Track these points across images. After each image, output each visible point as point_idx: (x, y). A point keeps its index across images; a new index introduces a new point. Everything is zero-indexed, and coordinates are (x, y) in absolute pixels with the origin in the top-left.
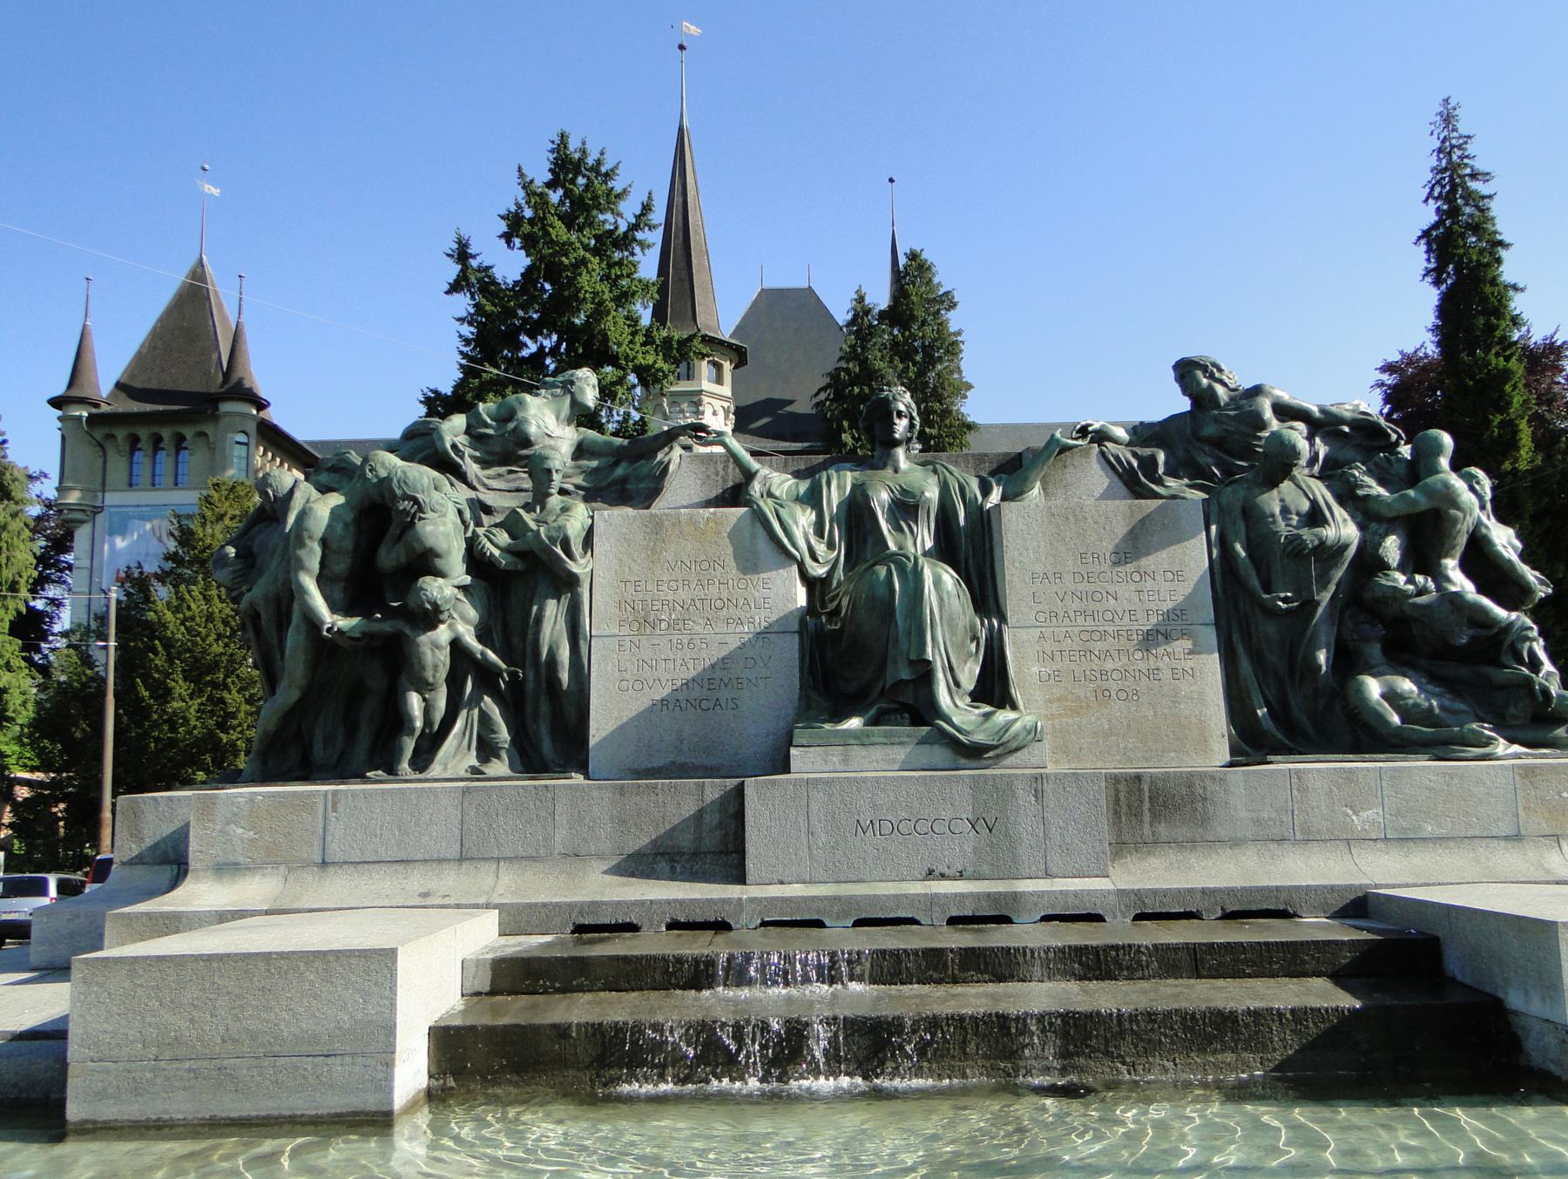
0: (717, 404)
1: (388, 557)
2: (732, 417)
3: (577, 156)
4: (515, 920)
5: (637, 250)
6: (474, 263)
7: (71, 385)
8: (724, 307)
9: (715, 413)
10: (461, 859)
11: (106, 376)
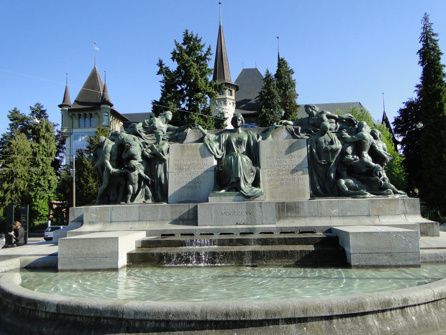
0: (231, 101)
1: (124, 156)
2: (235, 104)
3: (191, 36)
4: (149, 233)
5: (207, 61)
7: (63, 101)
8: (232, 75)
9: (230, 104)
10: (139, 221)
11: (72, 100)
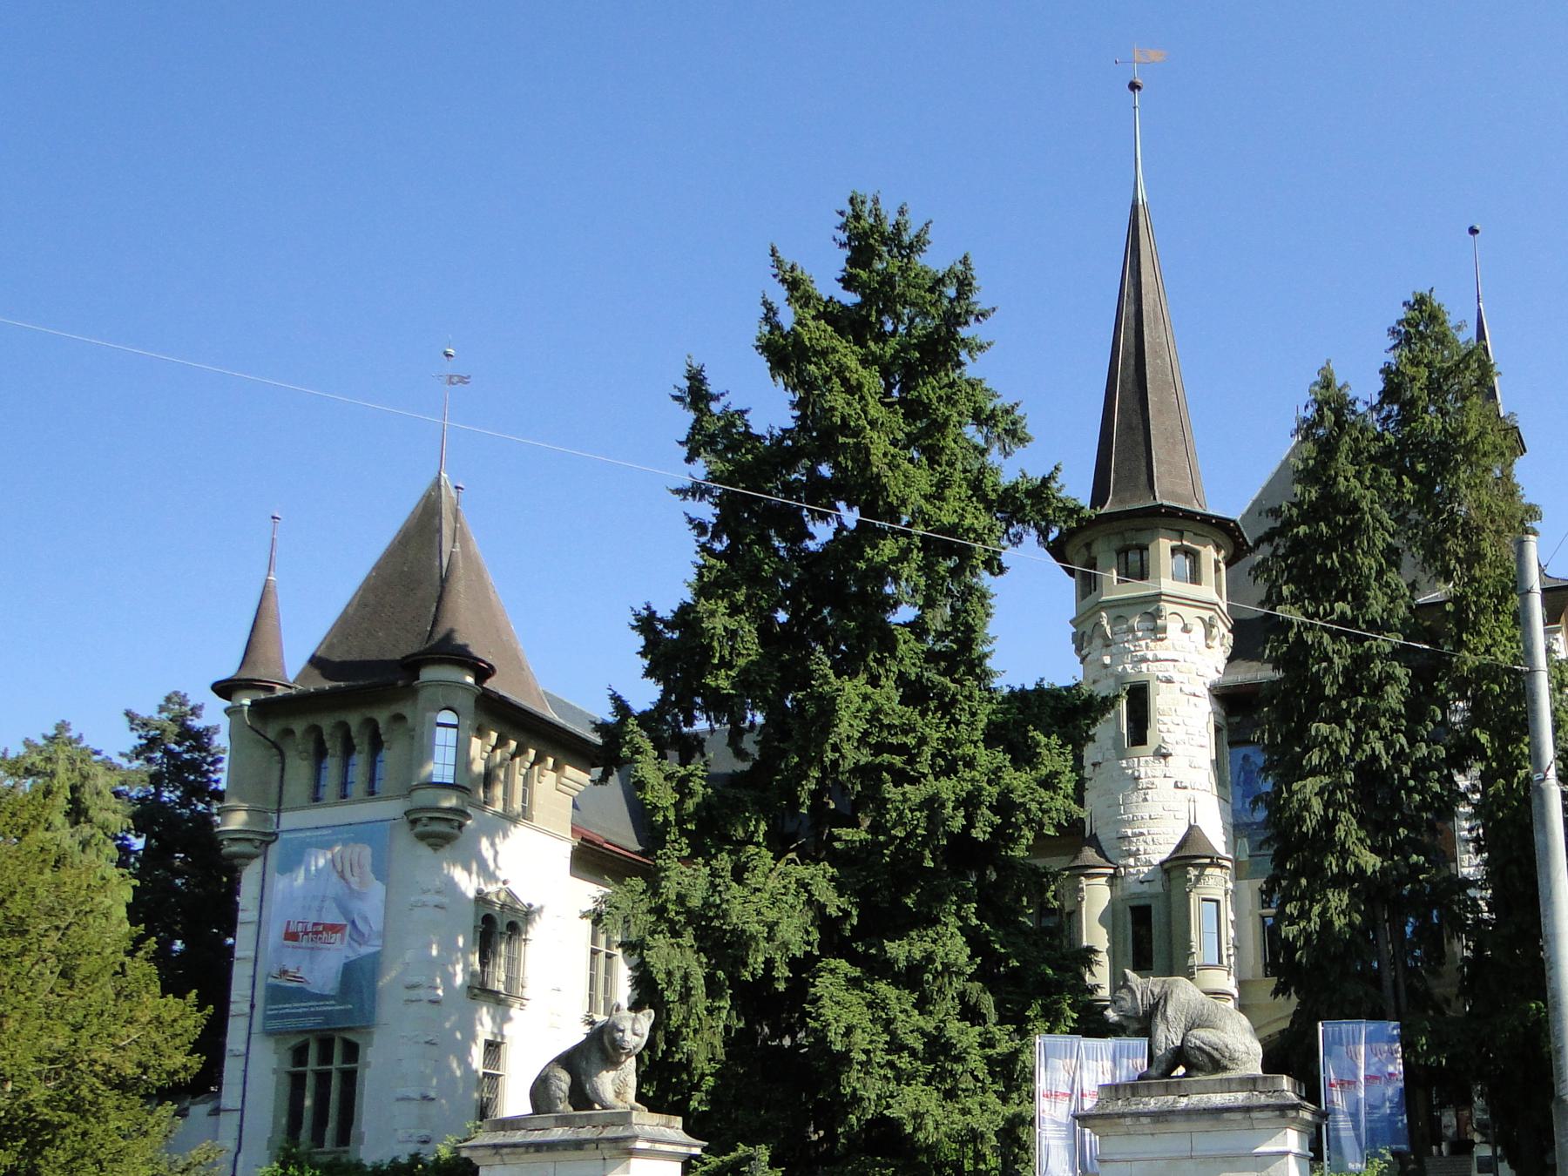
6: (715, 407)
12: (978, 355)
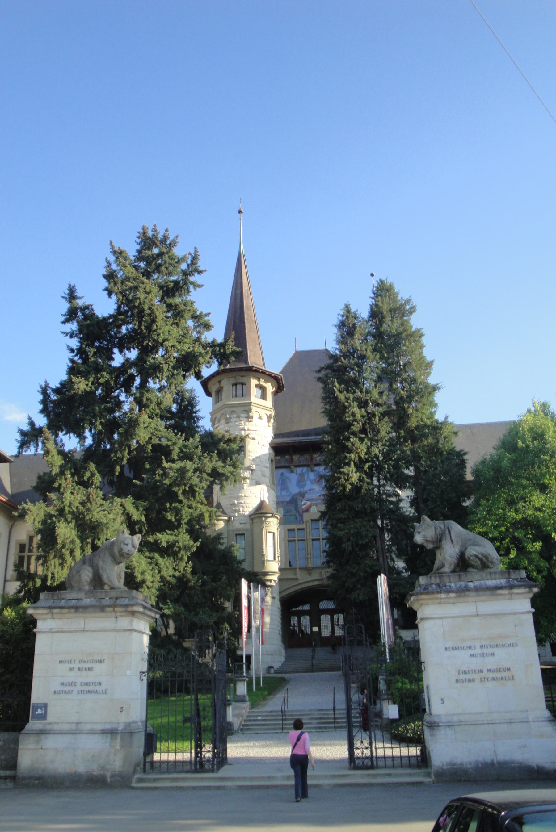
0: (263, 413)
2: (272, 421)
9: (260, 418)
12: (198, 289)
